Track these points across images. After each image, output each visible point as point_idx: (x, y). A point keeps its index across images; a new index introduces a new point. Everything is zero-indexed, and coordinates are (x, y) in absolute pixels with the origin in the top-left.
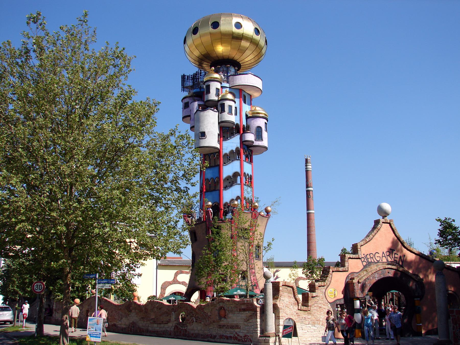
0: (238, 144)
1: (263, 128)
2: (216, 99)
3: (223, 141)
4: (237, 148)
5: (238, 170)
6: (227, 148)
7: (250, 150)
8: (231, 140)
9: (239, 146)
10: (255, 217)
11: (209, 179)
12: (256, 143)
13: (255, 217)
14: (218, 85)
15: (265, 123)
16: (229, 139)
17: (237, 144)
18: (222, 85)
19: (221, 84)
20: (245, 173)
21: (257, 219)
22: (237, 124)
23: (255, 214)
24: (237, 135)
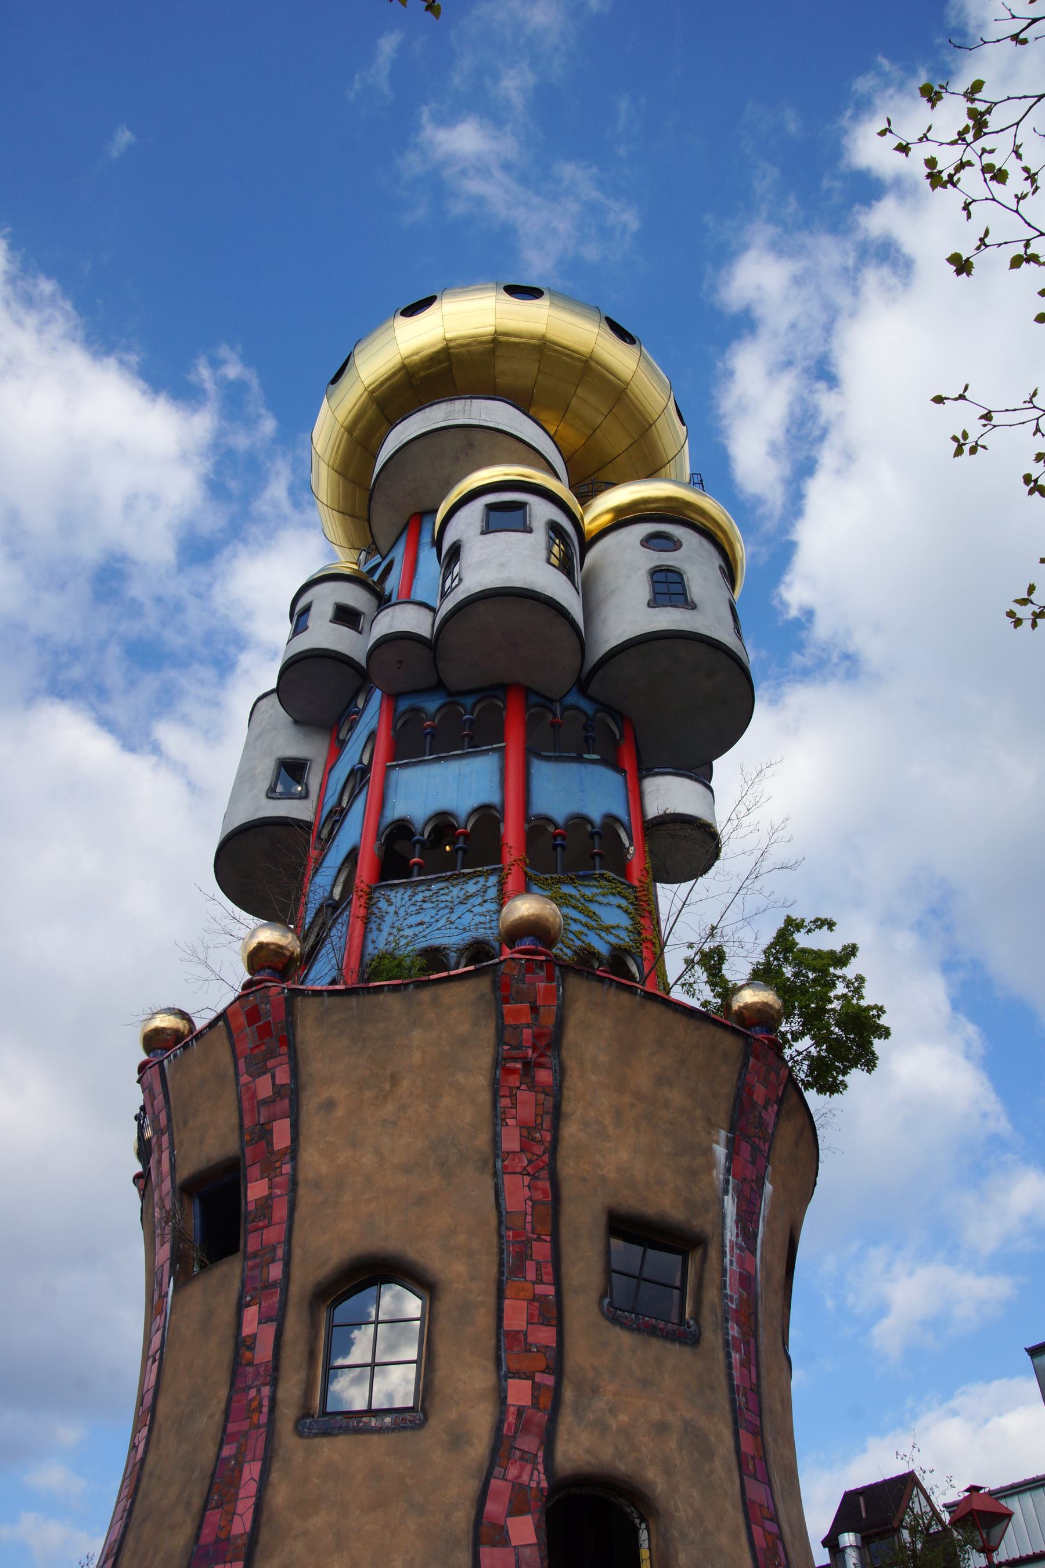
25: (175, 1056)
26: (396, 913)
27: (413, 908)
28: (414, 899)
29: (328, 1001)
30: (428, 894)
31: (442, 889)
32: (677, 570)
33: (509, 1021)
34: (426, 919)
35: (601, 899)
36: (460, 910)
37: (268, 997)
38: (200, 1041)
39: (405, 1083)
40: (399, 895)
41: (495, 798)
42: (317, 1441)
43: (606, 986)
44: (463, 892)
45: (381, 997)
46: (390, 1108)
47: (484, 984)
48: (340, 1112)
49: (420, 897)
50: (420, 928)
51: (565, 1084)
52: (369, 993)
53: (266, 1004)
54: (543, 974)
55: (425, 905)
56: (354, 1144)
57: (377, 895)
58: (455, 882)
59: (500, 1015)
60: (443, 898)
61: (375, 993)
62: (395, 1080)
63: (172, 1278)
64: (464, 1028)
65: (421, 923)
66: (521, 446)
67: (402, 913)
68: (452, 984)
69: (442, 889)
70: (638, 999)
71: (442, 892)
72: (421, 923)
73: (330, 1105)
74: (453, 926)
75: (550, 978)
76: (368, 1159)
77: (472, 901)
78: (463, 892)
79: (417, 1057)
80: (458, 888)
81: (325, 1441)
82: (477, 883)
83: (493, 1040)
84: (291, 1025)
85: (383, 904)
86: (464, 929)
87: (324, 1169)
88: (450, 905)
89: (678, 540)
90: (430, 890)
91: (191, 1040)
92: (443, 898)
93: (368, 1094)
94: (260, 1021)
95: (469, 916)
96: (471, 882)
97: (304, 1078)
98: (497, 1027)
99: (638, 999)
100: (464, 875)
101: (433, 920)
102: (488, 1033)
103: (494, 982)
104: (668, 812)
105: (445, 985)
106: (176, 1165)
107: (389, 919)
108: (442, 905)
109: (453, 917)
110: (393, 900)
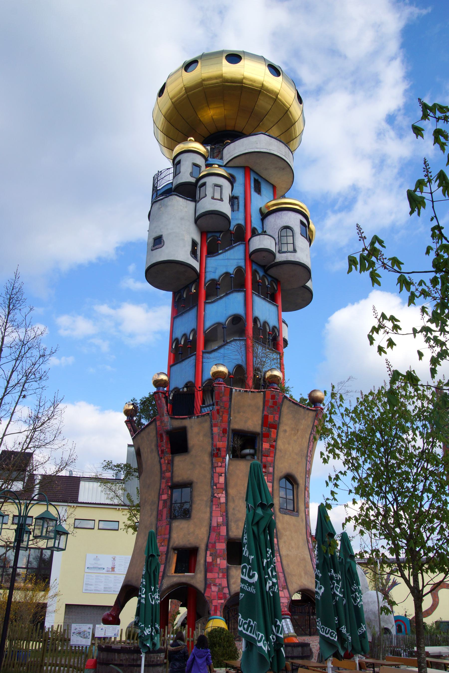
0: (239, 261)
1: (297, 229)
2: (193, 180)
3: (207, 257)
4: (239, 270)
5: (240, 311)
6: (216, 269)
7: (271, 276)
8: (224, 254)
9: (242, 263)
10: (275, 403)
11: (180, 338)
12: (280, 258)
13: (275, 403)
14: (200, 161)
15: (302, 222)
16: (220, 252)
17: (236, 261)
18: (208, 162)
19: (206, 160)
20: (256, 320)
22: (239, 226)
23: (273, 397)
24: (239, 245)
25: (240, 391)
38: (252, 393)
39: (299, 432)
42: (284, 515)
45: (301, 408)
46: (296, 437)
48: (287, 434)
56: (289, 444)
62: (298, 430)
64: (310, 423)
73: (285, 431)
76: (291, 449)
79: (302, 427)
81: (285, 515)
84: (282, 405)
87: (282, 447)
93: (293, 432)
97: (281, 421)
100: (273, 350)
106: (231, 422)
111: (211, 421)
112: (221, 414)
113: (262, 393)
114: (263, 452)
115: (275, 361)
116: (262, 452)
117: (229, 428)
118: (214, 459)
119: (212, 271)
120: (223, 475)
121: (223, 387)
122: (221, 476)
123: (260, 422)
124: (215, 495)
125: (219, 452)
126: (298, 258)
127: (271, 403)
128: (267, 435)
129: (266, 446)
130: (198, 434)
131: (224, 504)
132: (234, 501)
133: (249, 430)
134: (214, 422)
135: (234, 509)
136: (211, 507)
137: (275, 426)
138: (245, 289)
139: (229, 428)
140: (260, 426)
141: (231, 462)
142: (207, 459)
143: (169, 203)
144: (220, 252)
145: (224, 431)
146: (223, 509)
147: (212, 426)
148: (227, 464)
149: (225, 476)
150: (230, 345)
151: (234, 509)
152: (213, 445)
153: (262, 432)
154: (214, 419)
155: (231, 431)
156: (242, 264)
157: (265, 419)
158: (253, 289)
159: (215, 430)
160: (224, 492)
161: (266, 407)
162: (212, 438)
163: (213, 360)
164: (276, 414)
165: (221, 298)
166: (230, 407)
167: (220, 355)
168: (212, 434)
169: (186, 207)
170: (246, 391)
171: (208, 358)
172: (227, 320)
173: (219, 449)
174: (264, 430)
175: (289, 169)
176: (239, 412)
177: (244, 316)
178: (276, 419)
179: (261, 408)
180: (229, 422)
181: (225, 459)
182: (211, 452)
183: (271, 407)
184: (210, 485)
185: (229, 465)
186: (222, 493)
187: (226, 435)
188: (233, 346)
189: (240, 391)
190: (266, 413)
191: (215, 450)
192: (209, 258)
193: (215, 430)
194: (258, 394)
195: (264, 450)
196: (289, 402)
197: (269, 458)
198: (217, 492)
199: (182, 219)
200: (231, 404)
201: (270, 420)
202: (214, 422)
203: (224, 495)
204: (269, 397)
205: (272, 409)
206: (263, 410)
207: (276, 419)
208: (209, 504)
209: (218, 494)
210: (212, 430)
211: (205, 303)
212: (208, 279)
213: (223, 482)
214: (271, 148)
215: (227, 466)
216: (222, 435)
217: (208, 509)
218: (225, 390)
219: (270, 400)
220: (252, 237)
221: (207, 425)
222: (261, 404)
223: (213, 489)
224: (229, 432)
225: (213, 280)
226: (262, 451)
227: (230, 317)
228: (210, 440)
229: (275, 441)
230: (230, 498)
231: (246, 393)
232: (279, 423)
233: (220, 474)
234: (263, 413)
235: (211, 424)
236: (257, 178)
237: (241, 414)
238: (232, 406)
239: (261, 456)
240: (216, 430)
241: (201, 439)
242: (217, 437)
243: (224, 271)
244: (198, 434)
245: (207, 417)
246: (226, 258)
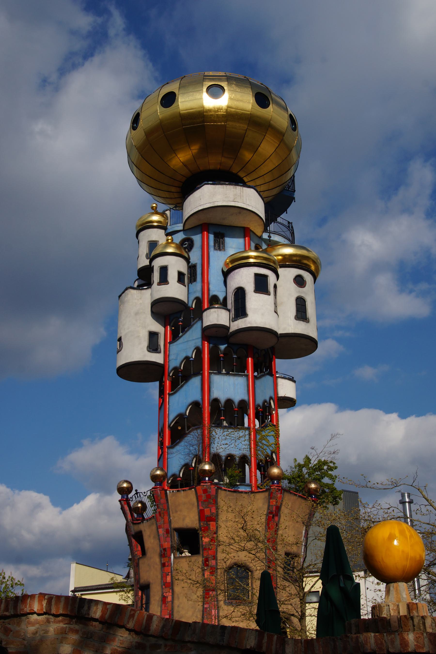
0: (197, 341)
3: (170, 343)
4: (199, 351)
5: (197, 397)
8: (184, 336)
9: (199, 343)
10: (209, 497)
13: (209, 497)
18: (169, 231)
20: (216, 401)
21: (215, 502)
24: (197, 322)
25: (173, 492)
26: (219, 438)
27: (224, 438)
28: (224, 434)
29: (228, 493)
30: (228, 433)
31: (232, 432)
32: (304, 299)
33: (271, 504)
34: (228, 443)
35: (269, 434)
36: (238, 441)
37: (211, 488)
38: (184, 492)
40: (219, 431)
41: (246, 398)
43: (292, 495)
44: (238, 435)
47: (267, 494)
49: (226, 433)
50: (226, 446)
51: (280, 520)
52: (239, 493)
53: (210, 489)
54: (280, 492)
55: (228, 437)
57: (212, 429)
58: (236, 430)
59: (269, 502)
60: (232, 435)
61: (241, 493)
63: (172, 554)
64: (261, 505)
65: (227, 444)
66: (258, 218)
67: (220, 438)
68: (260, 493)
69: (232, 432)
70: (297, 497)
71: (232, 433)
72: (227, 444)
74: (237, 447)
75: (281, 493)
77: (241, 439)
78: (238, 435)
80: (237, 433)
82: (242, 432)
83: (267, 509)
84: (217, 497)
85: (214, 433)
86: (240, 449)
88: (235, 439)
89: (305, 280)
90: (228, 431)
91: (181, 490)
92: (232, 435)
94: (207, 493)
95: (241, 445)
96: (241, 431)
98: (268, 505)
99: (297, 497)
101: (230, 444)
102: (266, 507)
103: (269, 494)
104: (286, 396)
105: (258, 493)
106: (172, 522)
107: (217, 440)
108: (233, 438)
109: (236, 444)
110: (217, 432)
111: (157, 524)
112: (162, 515)
113: (193, 490)
114: (204, 547)
115: (243, 439)
116: (202, 547)
117: (171, 528)
118: (162, 560)
119: (174, 358)
120: (170, 574)
121: (159, 491)
122: (168, 575)
123: (197, 517)
124: (165, 594)
125: (166, 553)
126: (249, 323)
127: (204, 497)
128: (207, 529)
129: (206, 540)
130: (150, 536)
131: (171, 602)
132: (179, 598)
133: (188, 527)
134: (159, 524)
135: (178, 606)
136: (161, 607)
137: (214, 518)
138: (201, 372)
139: (171, 528)
140: (198, 522)
141: (175, 560)
142: (157, 559)
143: (126, 299)
144: (180, 335)
145: (167, 531)
146: (170, 608)
147: (158, 528)
148: (172, 563)
149: (172, 575)
150: (189, 436)
151: (178, 606)
152: (161, 546)
153: (200, 527)
154: (158, 522)
155: (172, 531)
156: (199, 343)
157: (201, 513)
158: (210, 368)
159: (160, 530)
160: (171, 591)
161: (200, 503)
162: (159, 540)
163: (176, 454)
164: (212, 506)
165: (182, 386)
166: (168, 508)
167: (181, 448)
168: (159, 536)
169: (141, 299)
170: (178, 491)
171: (172, 453)
172: (187, 410)
173: (165, 550)
174: (202, 524)
175: (245, 211)
176: (176, 512)
177: (201, 402)
178: (214, 511)
179: (196, 504)
180: (170, 522)
181: (171, 558)
182: (160, 553)
183: (205, 501)
184: (160, 585)
185: (174, 564)
186: (169, 592)
187: (169, 536)
188: (191, 436)
189: (173, 492)
190: (201, 508)
191: (162, 550)
192: (172, 345)
193: (160, 530)
194: (189, 492)
195: (204, 544)
196: (225, 492)
197: (210, 552)
198: (166, 592)
199: (137, 314)
200: (168, 505)
201: (207, 513)
202: (159, 524)
203: (170, 594)
204: (200, 492)
205: (206, 503)
206: (198, 505)
207: (214, 511)
208: (160, 603)
209: (166, 593)
210: (158, 532)
211: (169, 395)
212: (171, 368)
213: (170, 581)
214: (214, 200)
215: (172, 565)
216: (166, 535)
217: (159, 608)
218: (160, 493)
219: (203, 495)
220: (208, 308)
221: (154, 527)
222: (194, 500)
223: (162, 588)
224: (171, 532)
225: (176, 369)
226: (202, 545)
227: (189, 405)
228: (158, 541)
229: (216, 533)
230: (176, 596)
231: (179, 492)
232: (217, 515)
233: (167, 573)
234: (198, 509)
235: (157, 526)
236: (218, 230)
237: (179, 513)
238: (170, 507)
239: (202, 551)
240: (161, 531)
241: (152, 541)
242: (163, 538)
243: (183, 355)
244: (150, 536)
245: (153, 520)
246: (186, 340)
